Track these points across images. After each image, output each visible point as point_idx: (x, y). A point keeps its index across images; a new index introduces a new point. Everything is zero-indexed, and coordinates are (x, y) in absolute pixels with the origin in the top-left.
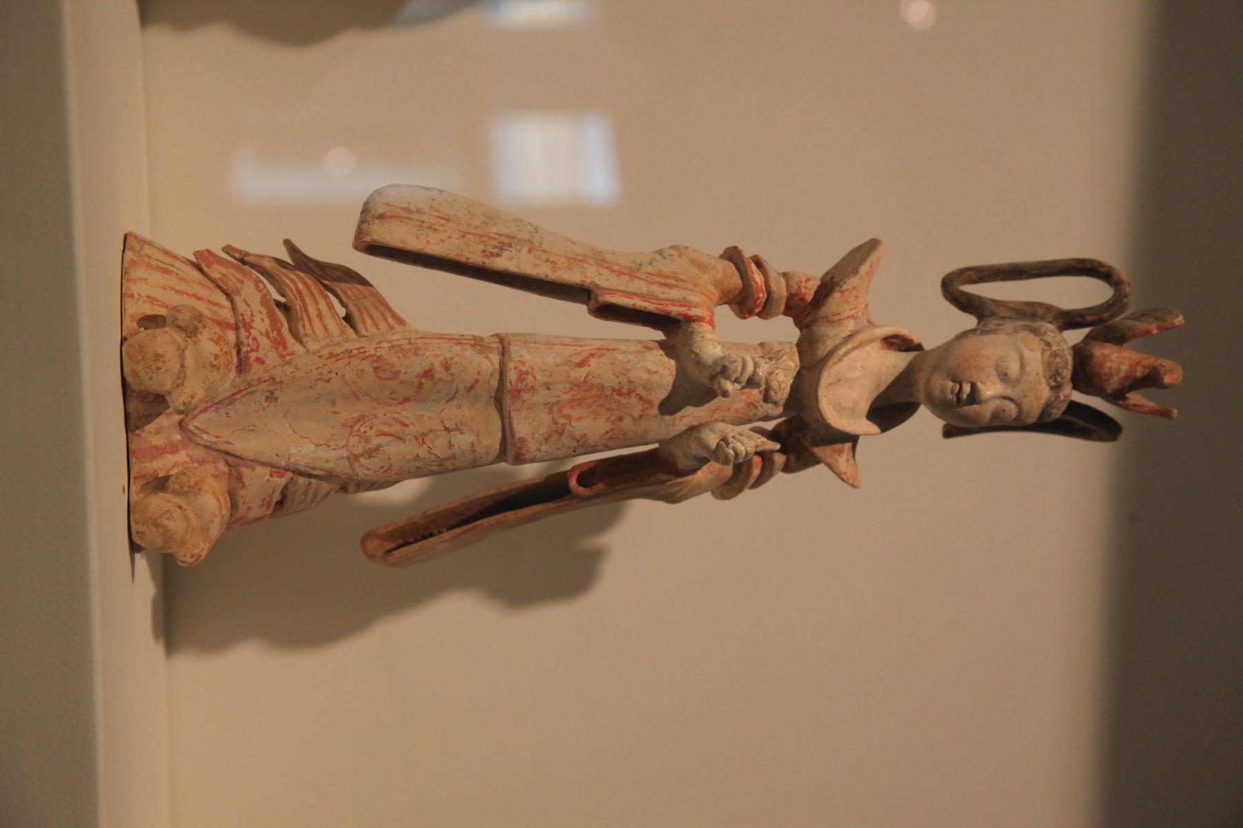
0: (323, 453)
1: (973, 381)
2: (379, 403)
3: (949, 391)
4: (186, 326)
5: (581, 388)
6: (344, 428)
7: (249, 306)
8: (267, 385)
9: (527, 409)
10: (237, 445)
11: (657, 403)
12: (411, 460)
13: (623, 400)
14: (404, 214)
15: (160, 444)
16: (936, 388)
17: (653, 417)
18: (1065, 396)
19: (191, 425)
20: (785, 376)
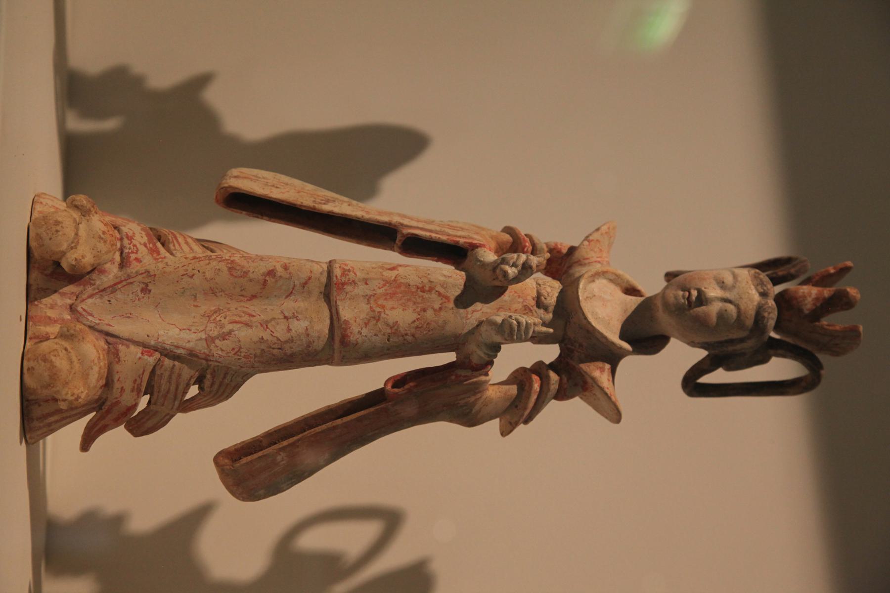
0: (185, 335)
1: (698, 287)
3: (682, 298)
8: (143, 278)
9: (350, 299)
10: (116, 327)
11: (452, 298)
12: (257, 342)
13: (426, 295)
14: (253, 178)
15: (54, 317)
17: (450, 309)
18: (772, 304)
19: (80, 307)
20: (552, 290)
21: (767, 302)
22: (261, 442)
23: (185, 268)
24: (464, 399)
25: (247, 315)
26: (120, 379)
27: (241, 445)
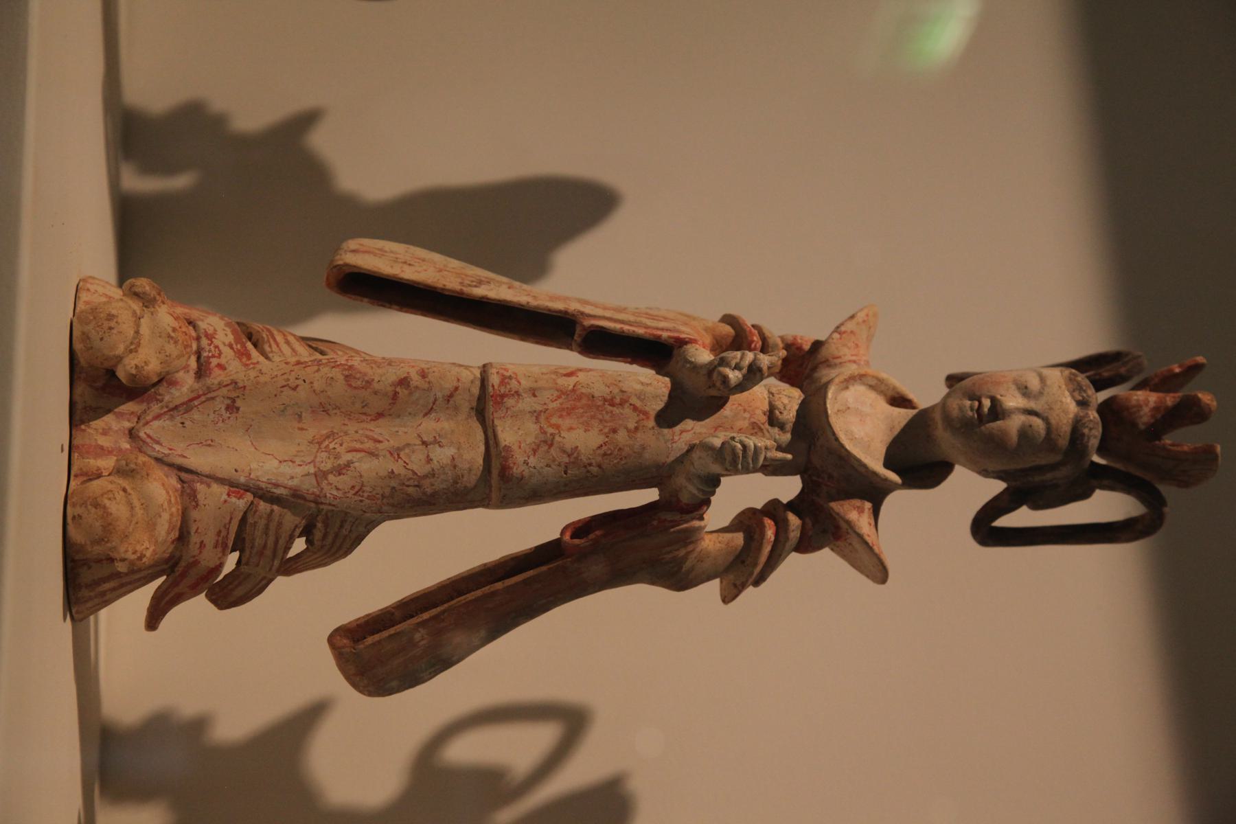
0: (287, 469)
1: (989, 394)
2: (349, 419)
3: (969, 410)
5: (570, 396)
6: (311, 445)
9: (511, 417)
11: (653, 414)
13: (616, 410)
14: (377, 252)
17: (650, 429)
18: (1094, 417)
20: (790, 402)
21: (1087, 414)
22: (393, 614)
23: (285, 376)
24: (670, 552)
25: (370, 441)
26: (199, 531)
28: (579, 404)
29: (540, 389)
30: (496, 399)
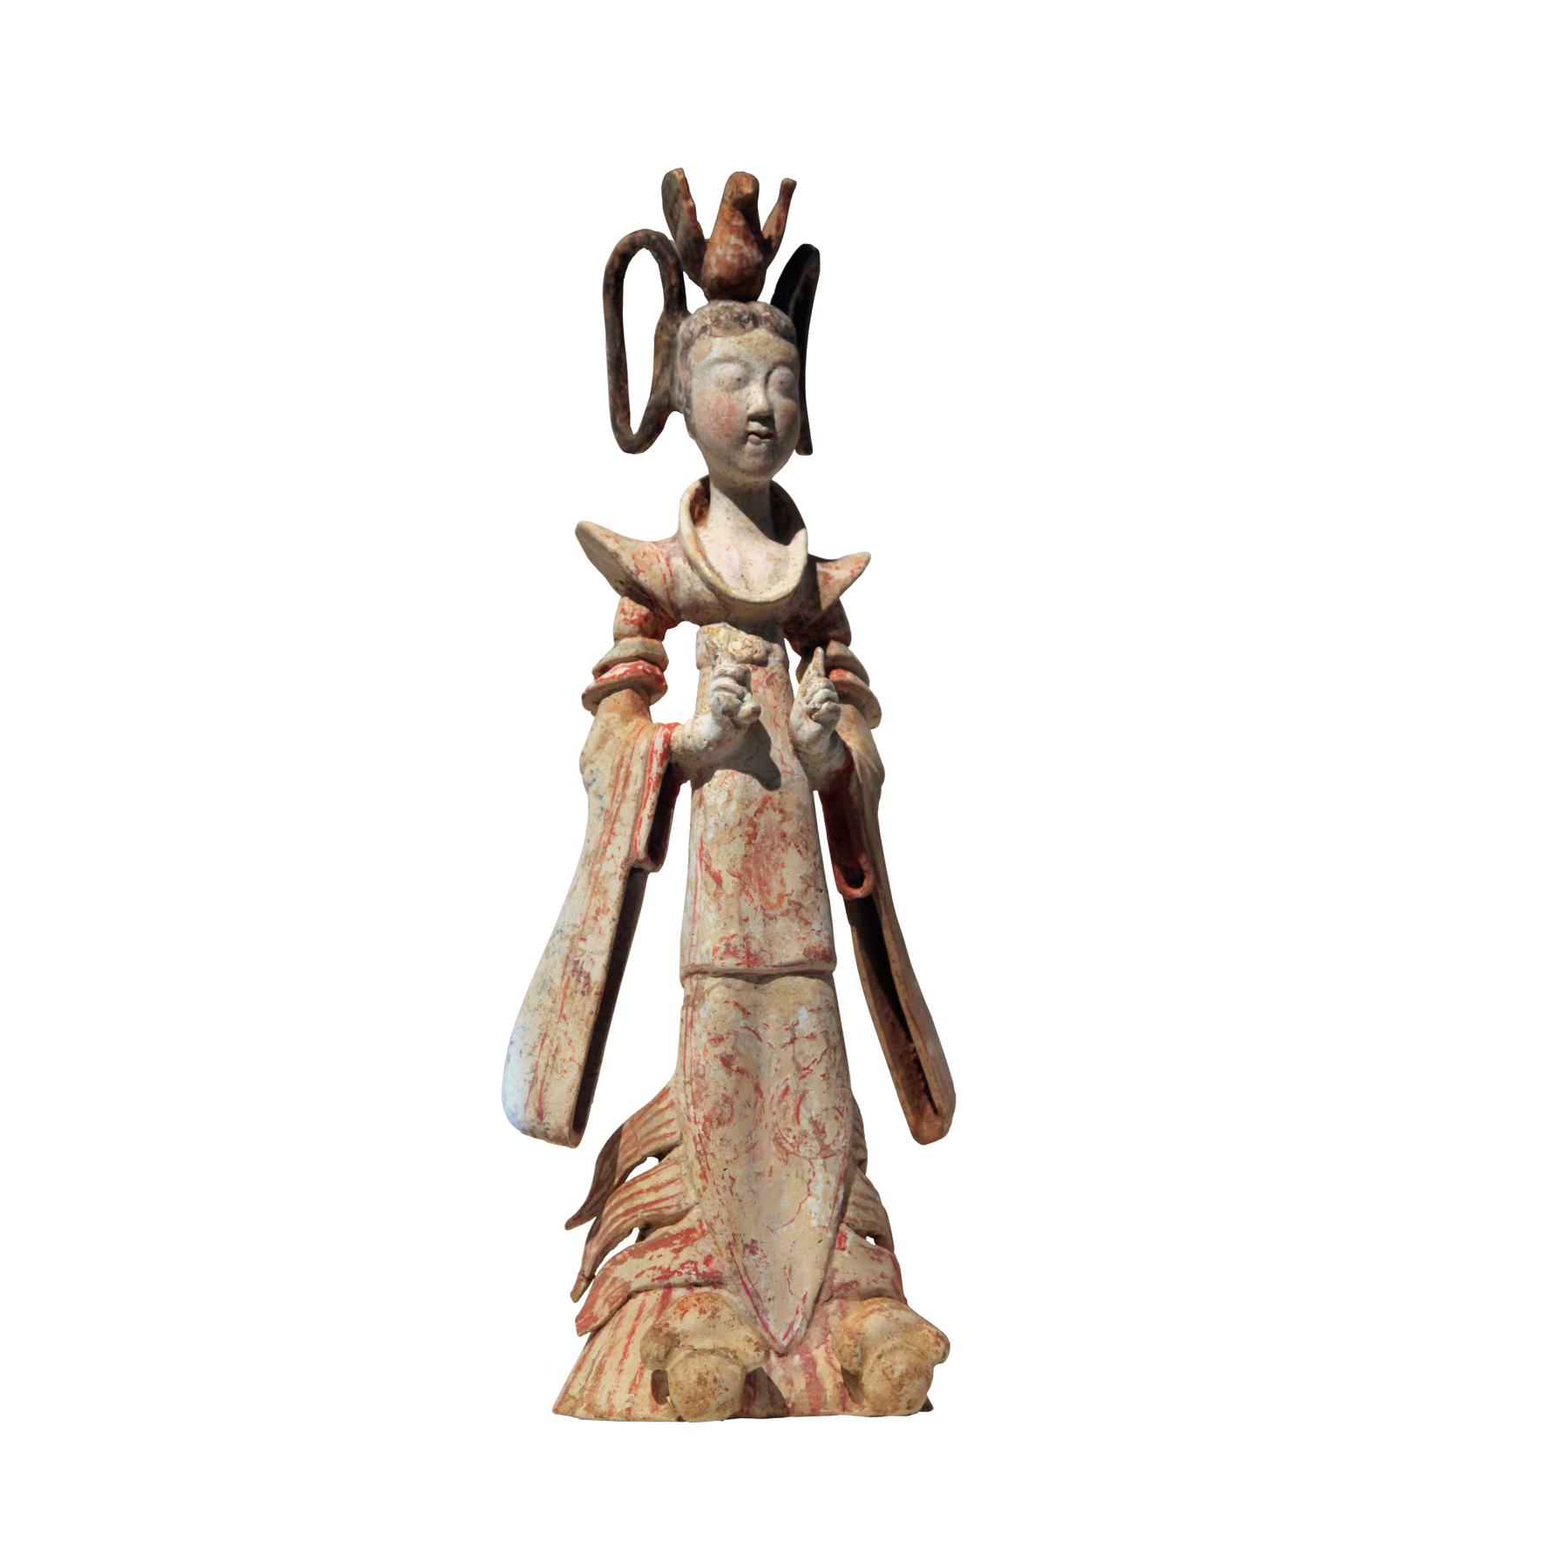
0: (819, 1188)
1: (745, 419)
2: (761, 1120)
3: (757, 447)
4: (666, 1346)
6: (790, 1162)
7: (643, 1272)
9: (770, 946)
11: (765, 792)
12: (828, 1083)
13: (761, 832)
16: (754, 462)
18: (766, 310)
20: (736, 640)
27: (907, 1105)
28: (754, 873)
29: (740, 914)
30: (751, 962)
